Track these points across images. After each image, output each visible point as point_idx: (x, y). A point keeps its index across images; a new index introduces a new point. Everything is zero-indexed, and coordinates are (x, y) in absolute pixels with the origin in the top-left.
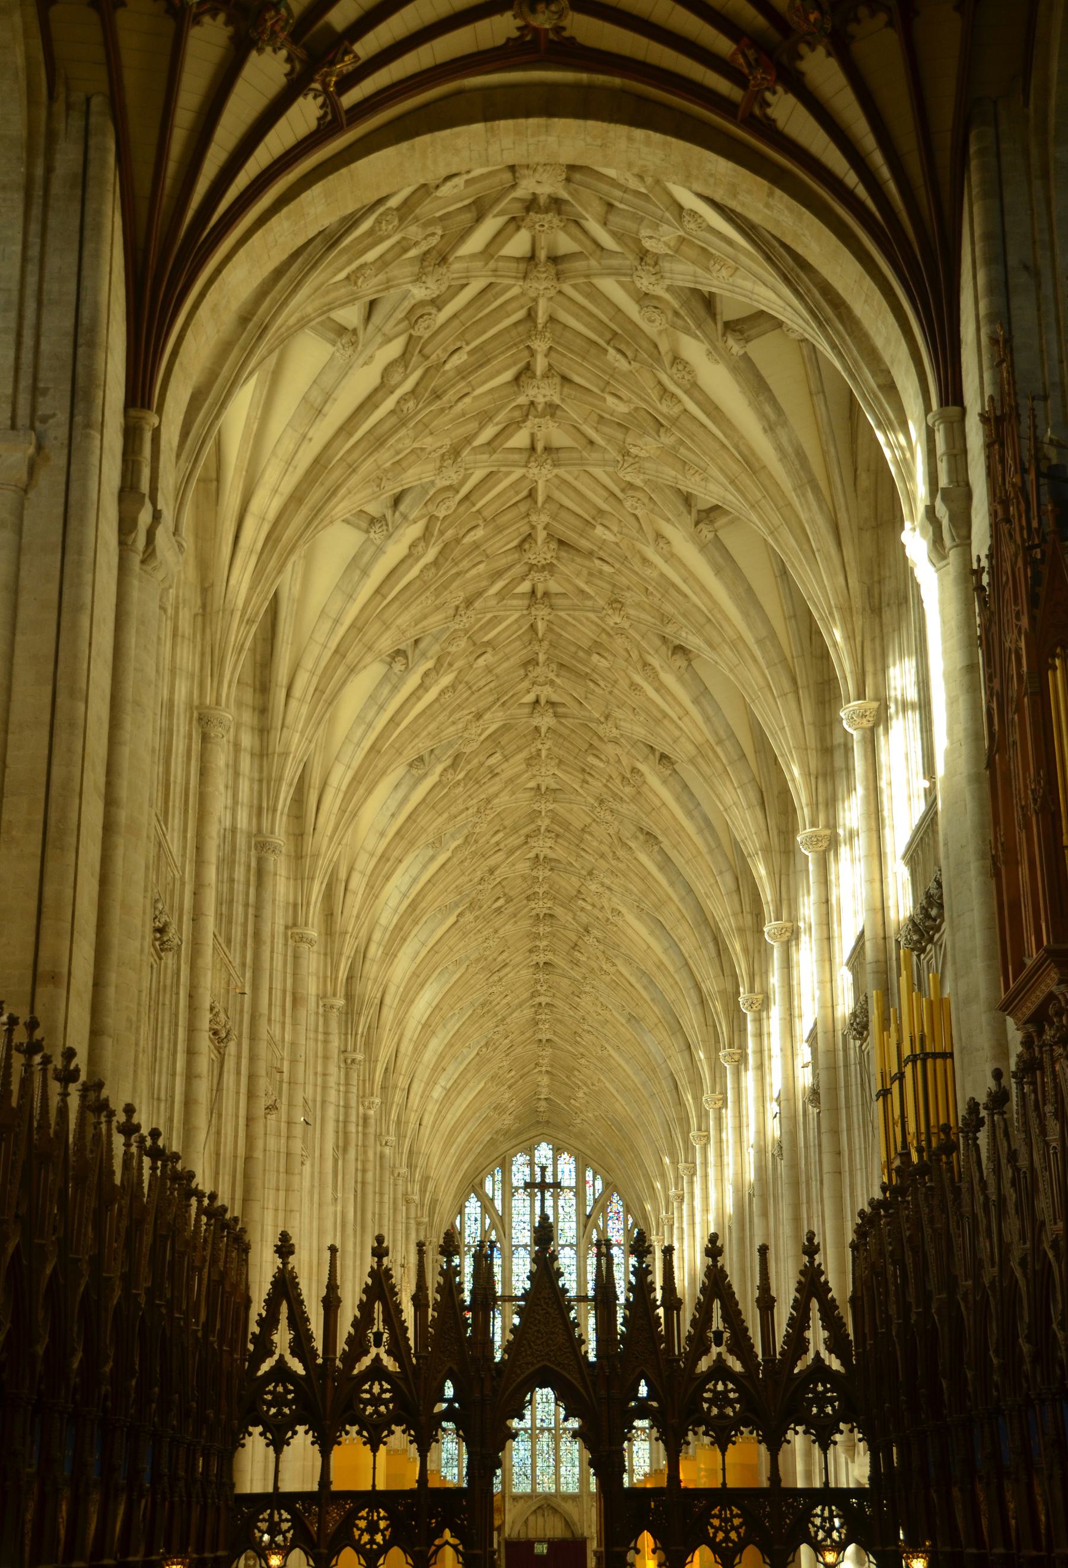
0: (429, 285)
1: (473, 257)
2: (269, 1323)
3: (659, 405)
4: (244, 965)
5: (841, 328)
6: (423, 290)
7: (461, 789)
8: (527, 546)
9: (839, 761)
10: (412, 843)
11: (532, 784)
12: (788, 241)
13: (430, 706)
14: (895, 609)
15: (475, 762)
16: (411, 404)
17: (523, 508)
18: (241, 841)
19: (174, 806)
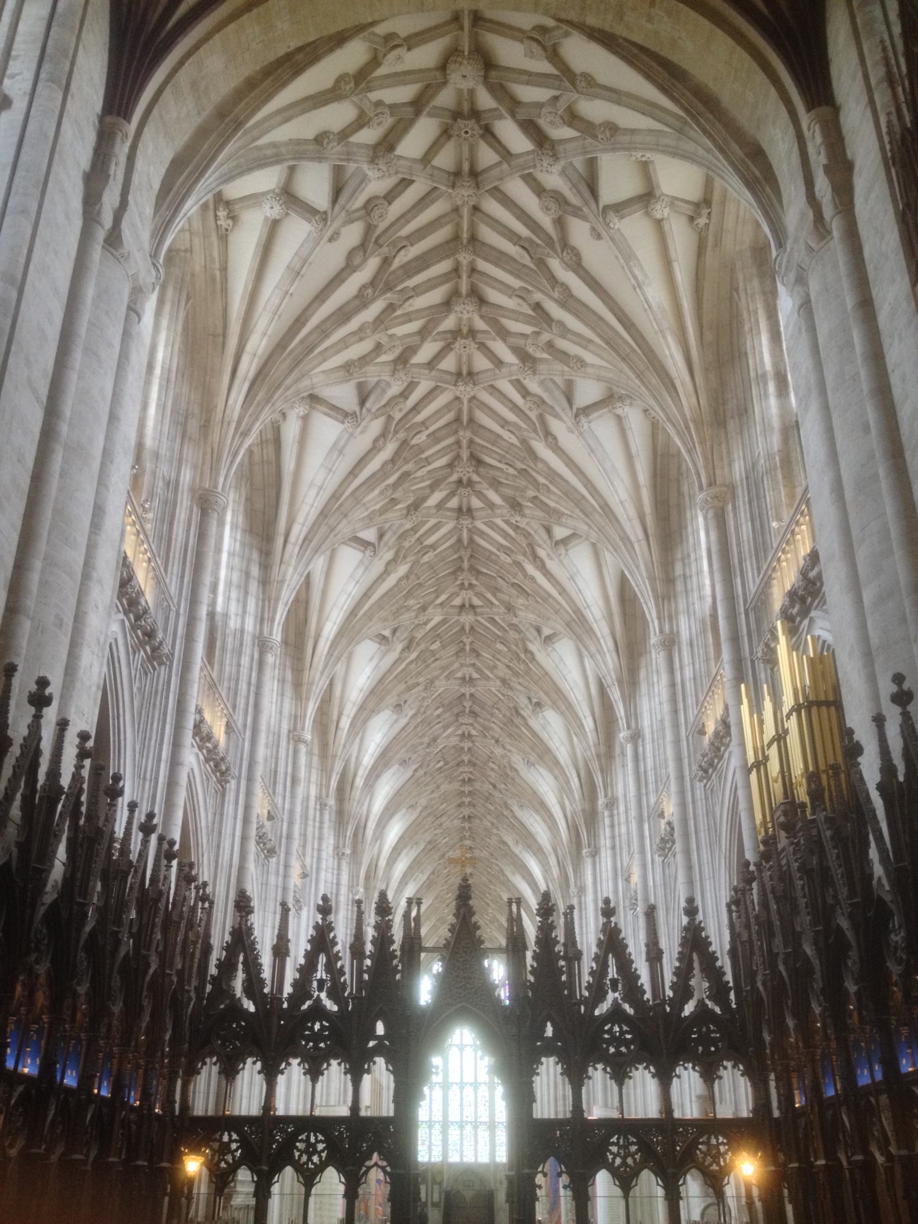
0: (381, 166)
1: (414, 160)
2: (227, 967)
3: (552, 293)
4: (245, 726)
5: (711, 117)
6: (376, 171)
7: (413, 666)
8: (456, 463)
9: (679, 586)
10: (382, 699)
11: (459, 675)
12: (665, 53)
13: (390, 590)
14: (737, 419)
15: (423, 646)
16: (370, 291)
17: (454, 426)
18: (248, 639)
19: (174, 557)
